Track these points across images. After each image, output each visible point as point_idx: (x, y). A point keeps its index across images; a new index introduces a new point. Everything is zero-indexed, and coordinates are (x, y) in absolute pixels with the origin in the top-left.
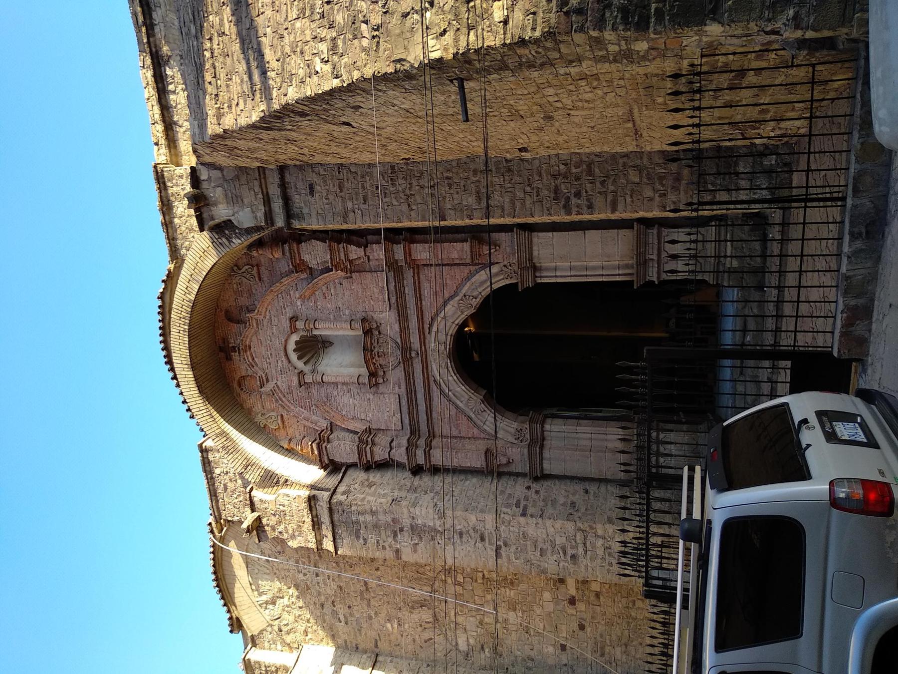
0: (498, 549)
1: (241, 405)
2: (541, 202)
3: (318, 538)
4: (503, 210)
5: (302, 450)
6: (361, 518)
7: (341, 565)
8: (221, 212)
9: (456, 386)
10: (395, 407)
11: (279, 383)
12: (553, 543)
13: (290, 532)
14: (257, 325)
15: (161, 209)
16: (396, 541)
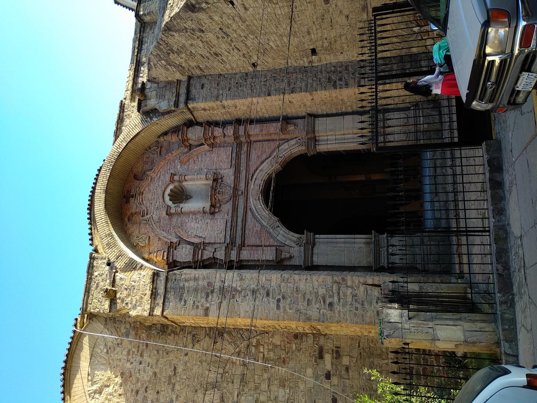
0: (278, 301)
1: (126, 232)
2: (321, 84)
3: (152, 306)
4: (301, 89)
5: (156, 257)
6: (187, 284)
7: (161, 352)
8: (152, 103)
9: (263, 211)
10: (223, 227)
11: (154, 216)
12: (317, 293)
13: (134, 303)
14: (151, 179)
15: (118, 121)
16: (207, 301)
